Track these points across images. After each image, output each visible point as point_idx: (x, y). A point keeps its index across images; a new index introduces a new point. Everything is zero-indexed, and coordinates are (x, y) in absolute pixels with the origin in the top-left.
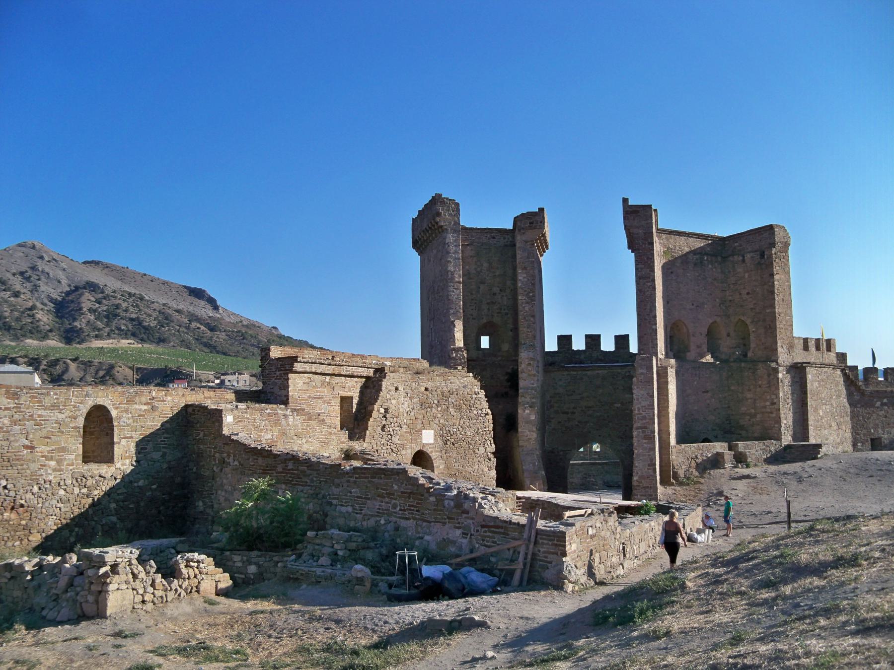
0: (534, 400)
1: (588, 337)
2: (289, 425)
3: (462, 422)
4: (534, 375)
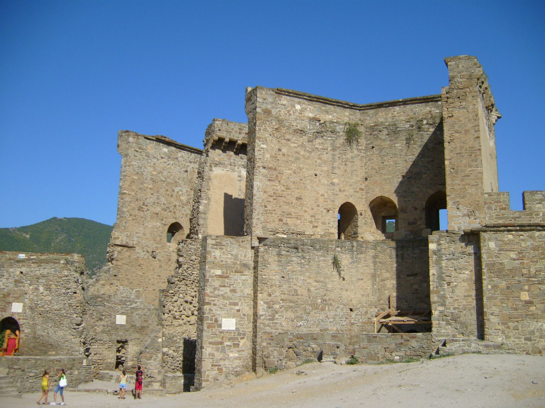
3: (50, 298)
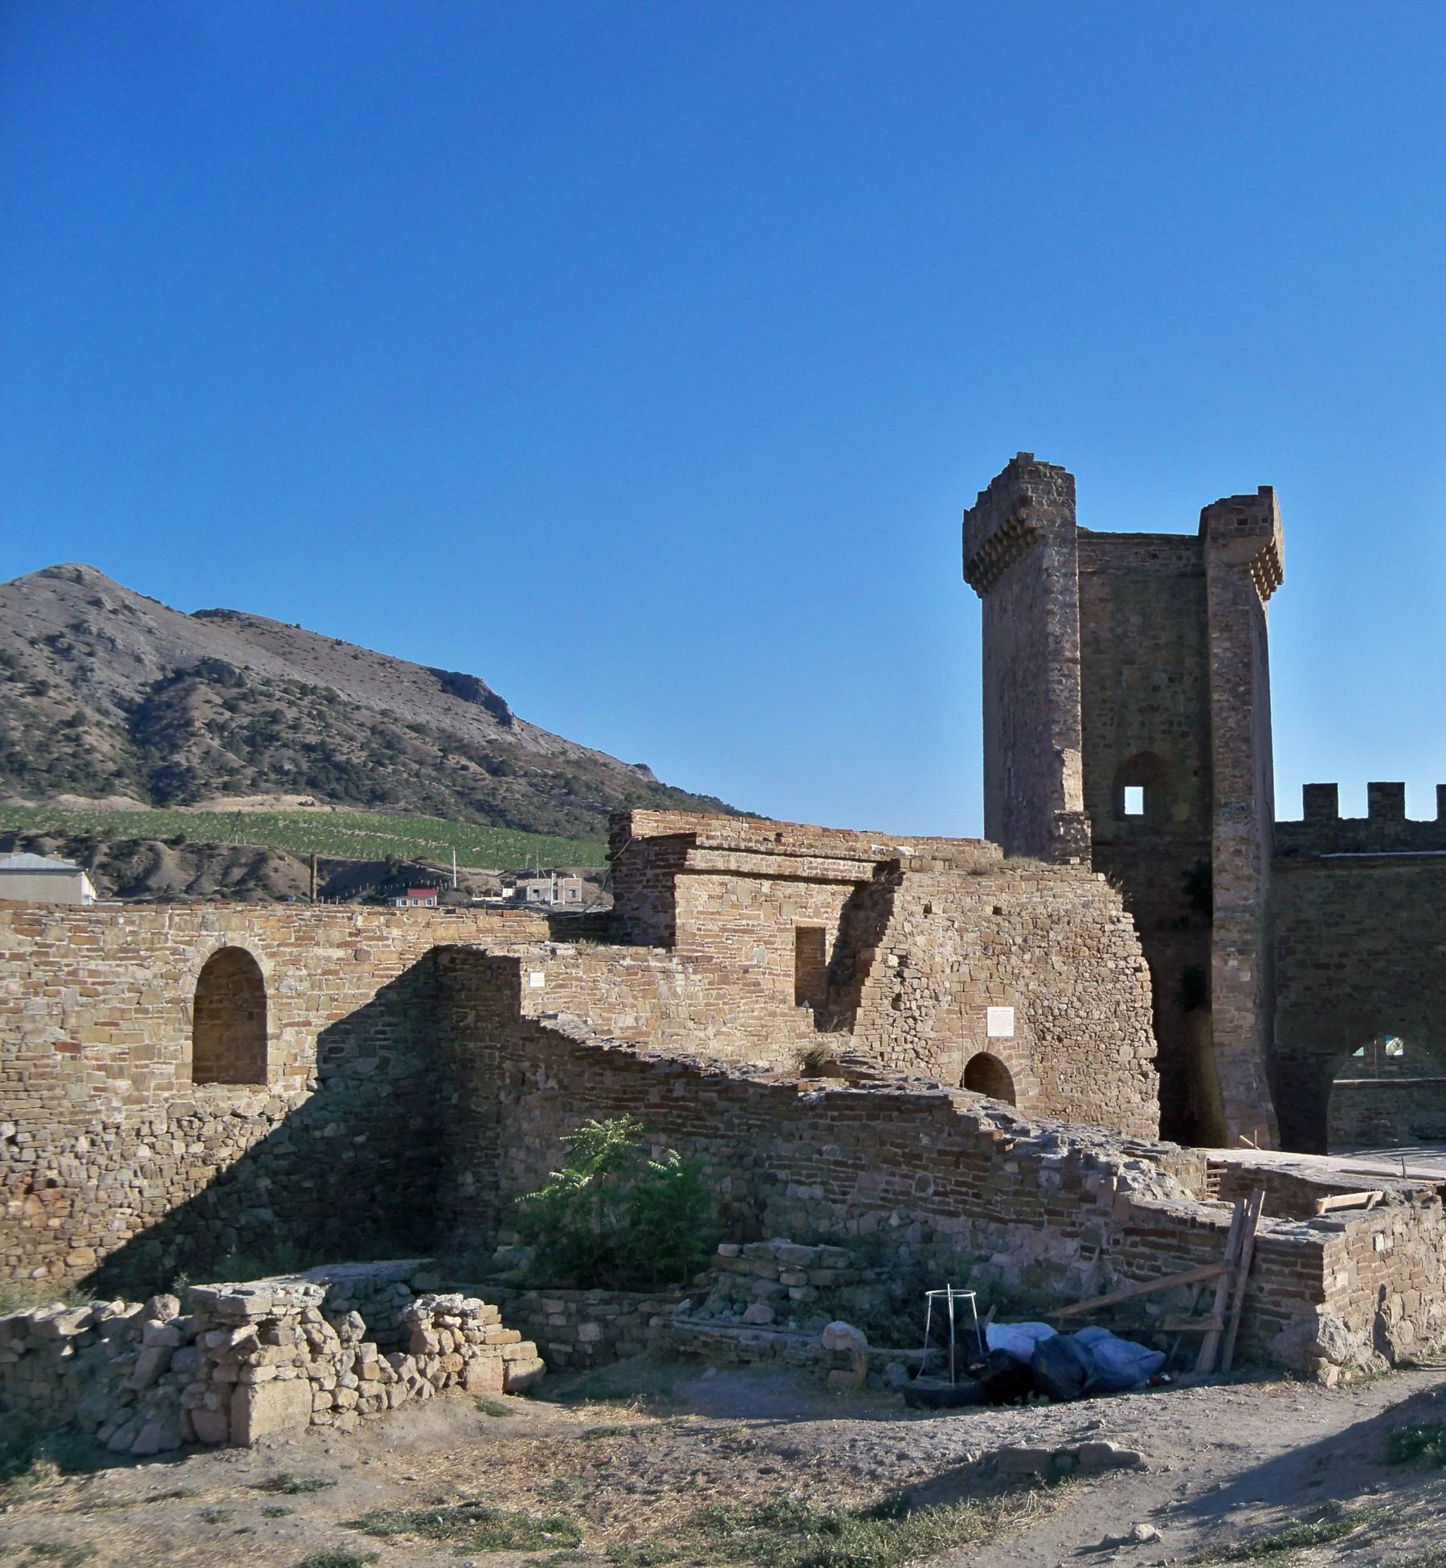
0: (1248, 937)
1: (1373, 788)
2: (675, 994)
3: (1080, 988)
4: (1249, 878)
